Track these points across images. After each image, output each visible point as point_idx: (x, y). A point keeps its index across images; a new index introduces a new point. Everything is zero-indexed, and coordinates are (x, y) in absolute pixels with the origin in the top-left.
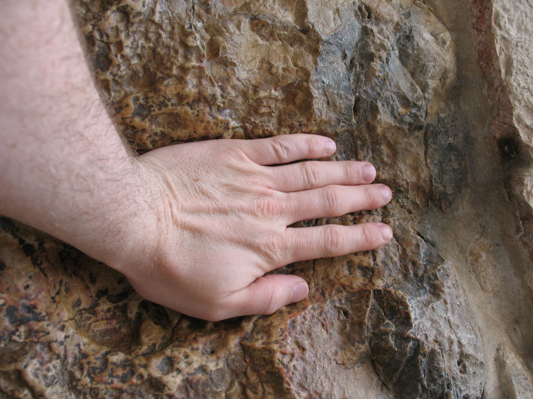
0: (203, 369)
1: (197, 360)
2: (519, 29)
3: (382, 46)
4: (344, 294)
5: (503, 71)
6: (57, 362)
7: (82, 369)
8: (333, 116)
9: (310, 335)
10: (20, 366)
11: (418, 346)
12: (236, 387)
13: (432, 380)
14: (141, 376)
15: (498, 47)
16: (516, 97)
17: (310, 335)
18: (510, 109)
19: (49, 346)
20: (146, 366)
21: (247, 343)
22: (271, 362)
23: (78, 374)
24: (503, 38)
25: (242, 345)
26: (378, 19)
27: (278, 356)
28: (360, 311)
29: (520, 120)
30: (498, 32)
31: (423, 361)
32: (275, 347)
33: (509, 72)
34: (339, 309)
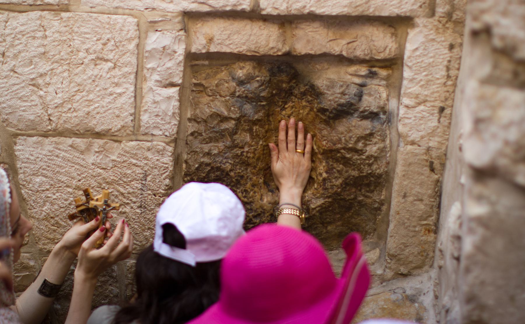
0: (324, 167)
1: (322, 168)
2: (244, 45)
3: (243, 92)
4: (316, 120)
5: (257, 54)
6: (313, 200)
7: (316, 195)
8: (263, 111)
9: (324, 137)
10: (311, 208)
11: (334, 109)
12: (330, 159)
13: (345, 106)
14: (321, 182)
15: (249, 54)
16: (267, 53)
17: (324, 137)
18: (270, 55)
19: (308, 201)
20: (319, 180)
21: (321, 153)
22: (326, 150)
23: (317, 196)
24: (246, 52)
25: (321, 154)
26: (235, 92)
27: (326, 148)
28: (321, 118)
29: (274, 53)
30: (244, 52)
31: (339, 108)
32: (323, 148)
33: (258, 53)
34: (320, 123)
